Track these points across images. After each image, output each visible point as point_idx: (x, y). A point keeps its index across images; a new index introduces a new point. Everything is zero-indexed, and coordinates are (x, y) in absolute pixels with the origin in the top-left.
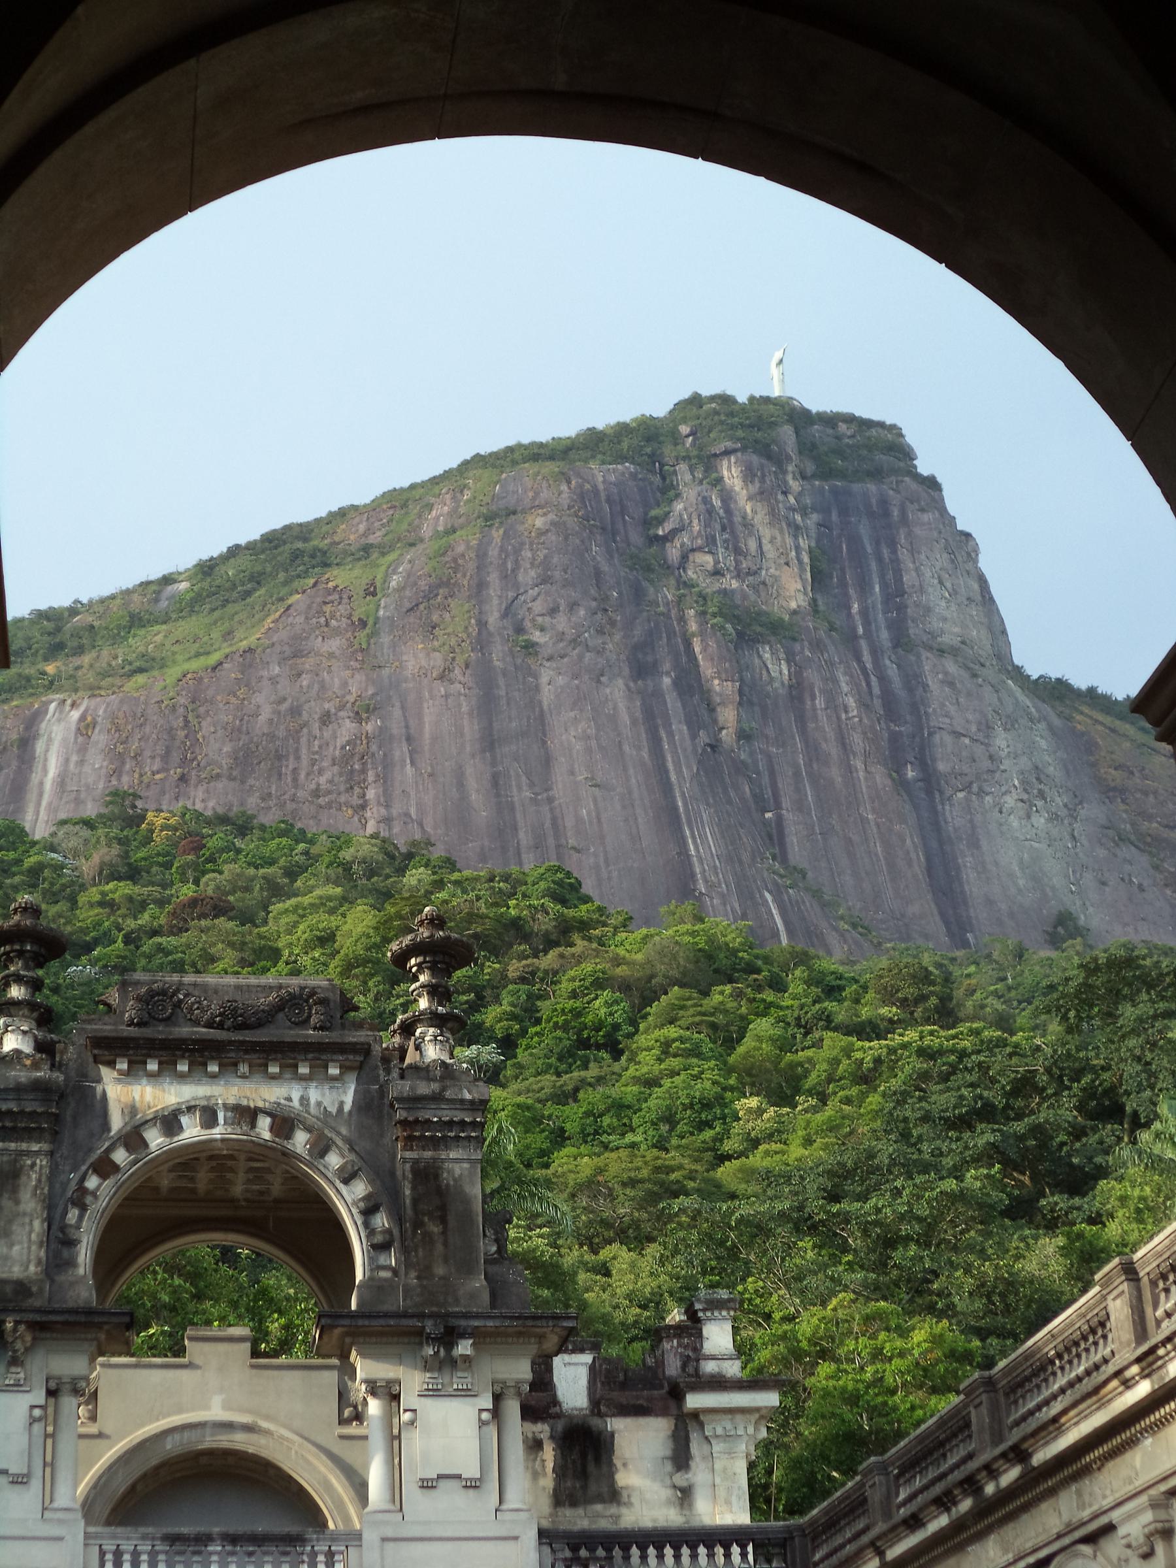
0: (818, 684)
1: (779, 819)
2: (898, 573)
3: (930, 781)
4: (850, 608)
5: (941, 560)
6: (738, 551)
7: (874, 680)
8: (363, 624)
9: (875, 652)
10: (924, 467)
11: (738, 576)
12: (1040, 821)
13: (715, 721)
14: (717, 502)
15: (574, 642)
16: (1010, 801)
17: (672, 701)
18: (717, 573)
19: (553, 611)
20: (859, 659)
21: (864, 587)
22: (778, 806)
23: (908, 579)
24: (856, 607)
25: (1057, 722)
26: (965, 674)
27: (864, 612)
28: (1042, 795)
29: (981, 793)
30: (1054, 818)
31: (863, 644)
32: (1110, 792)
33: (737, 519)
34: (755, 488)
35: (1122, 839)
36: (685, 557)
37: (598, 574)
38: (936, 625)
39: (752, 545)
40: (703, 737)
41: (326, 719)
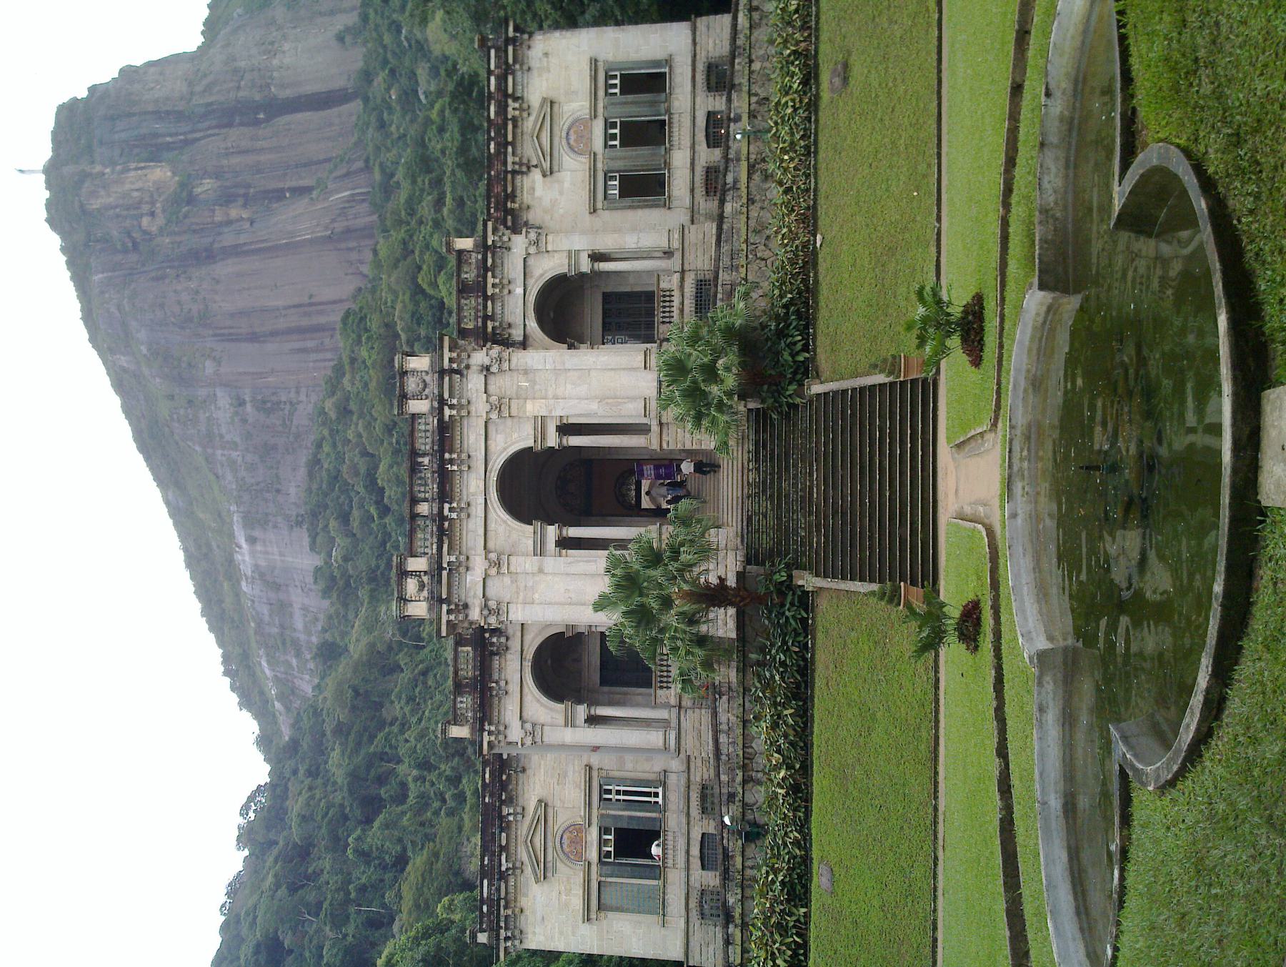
1: (289, 189)
6: (140, 202)
7: (210, 132)
8: (190, 402)
11: (153, 203)
12: (286, 46)
13: (237, 220)
14: (111, 212)
15: (197, 292)
16: (275, 62)
18: (152, 214)
19: (179, 302)
21: (156, 135)
22: (282, 191)
23: (150, 108)
24: (169, 139)
27: (171, 135)
28: (272, 43)
29: (271, 78)
30: (285, 37)
31: (190, 136)
33: (121, 202)
34: (102, 193)
36: (145, 232)
39: (135, 194)
40: (247, 225)
41: (244, 421)
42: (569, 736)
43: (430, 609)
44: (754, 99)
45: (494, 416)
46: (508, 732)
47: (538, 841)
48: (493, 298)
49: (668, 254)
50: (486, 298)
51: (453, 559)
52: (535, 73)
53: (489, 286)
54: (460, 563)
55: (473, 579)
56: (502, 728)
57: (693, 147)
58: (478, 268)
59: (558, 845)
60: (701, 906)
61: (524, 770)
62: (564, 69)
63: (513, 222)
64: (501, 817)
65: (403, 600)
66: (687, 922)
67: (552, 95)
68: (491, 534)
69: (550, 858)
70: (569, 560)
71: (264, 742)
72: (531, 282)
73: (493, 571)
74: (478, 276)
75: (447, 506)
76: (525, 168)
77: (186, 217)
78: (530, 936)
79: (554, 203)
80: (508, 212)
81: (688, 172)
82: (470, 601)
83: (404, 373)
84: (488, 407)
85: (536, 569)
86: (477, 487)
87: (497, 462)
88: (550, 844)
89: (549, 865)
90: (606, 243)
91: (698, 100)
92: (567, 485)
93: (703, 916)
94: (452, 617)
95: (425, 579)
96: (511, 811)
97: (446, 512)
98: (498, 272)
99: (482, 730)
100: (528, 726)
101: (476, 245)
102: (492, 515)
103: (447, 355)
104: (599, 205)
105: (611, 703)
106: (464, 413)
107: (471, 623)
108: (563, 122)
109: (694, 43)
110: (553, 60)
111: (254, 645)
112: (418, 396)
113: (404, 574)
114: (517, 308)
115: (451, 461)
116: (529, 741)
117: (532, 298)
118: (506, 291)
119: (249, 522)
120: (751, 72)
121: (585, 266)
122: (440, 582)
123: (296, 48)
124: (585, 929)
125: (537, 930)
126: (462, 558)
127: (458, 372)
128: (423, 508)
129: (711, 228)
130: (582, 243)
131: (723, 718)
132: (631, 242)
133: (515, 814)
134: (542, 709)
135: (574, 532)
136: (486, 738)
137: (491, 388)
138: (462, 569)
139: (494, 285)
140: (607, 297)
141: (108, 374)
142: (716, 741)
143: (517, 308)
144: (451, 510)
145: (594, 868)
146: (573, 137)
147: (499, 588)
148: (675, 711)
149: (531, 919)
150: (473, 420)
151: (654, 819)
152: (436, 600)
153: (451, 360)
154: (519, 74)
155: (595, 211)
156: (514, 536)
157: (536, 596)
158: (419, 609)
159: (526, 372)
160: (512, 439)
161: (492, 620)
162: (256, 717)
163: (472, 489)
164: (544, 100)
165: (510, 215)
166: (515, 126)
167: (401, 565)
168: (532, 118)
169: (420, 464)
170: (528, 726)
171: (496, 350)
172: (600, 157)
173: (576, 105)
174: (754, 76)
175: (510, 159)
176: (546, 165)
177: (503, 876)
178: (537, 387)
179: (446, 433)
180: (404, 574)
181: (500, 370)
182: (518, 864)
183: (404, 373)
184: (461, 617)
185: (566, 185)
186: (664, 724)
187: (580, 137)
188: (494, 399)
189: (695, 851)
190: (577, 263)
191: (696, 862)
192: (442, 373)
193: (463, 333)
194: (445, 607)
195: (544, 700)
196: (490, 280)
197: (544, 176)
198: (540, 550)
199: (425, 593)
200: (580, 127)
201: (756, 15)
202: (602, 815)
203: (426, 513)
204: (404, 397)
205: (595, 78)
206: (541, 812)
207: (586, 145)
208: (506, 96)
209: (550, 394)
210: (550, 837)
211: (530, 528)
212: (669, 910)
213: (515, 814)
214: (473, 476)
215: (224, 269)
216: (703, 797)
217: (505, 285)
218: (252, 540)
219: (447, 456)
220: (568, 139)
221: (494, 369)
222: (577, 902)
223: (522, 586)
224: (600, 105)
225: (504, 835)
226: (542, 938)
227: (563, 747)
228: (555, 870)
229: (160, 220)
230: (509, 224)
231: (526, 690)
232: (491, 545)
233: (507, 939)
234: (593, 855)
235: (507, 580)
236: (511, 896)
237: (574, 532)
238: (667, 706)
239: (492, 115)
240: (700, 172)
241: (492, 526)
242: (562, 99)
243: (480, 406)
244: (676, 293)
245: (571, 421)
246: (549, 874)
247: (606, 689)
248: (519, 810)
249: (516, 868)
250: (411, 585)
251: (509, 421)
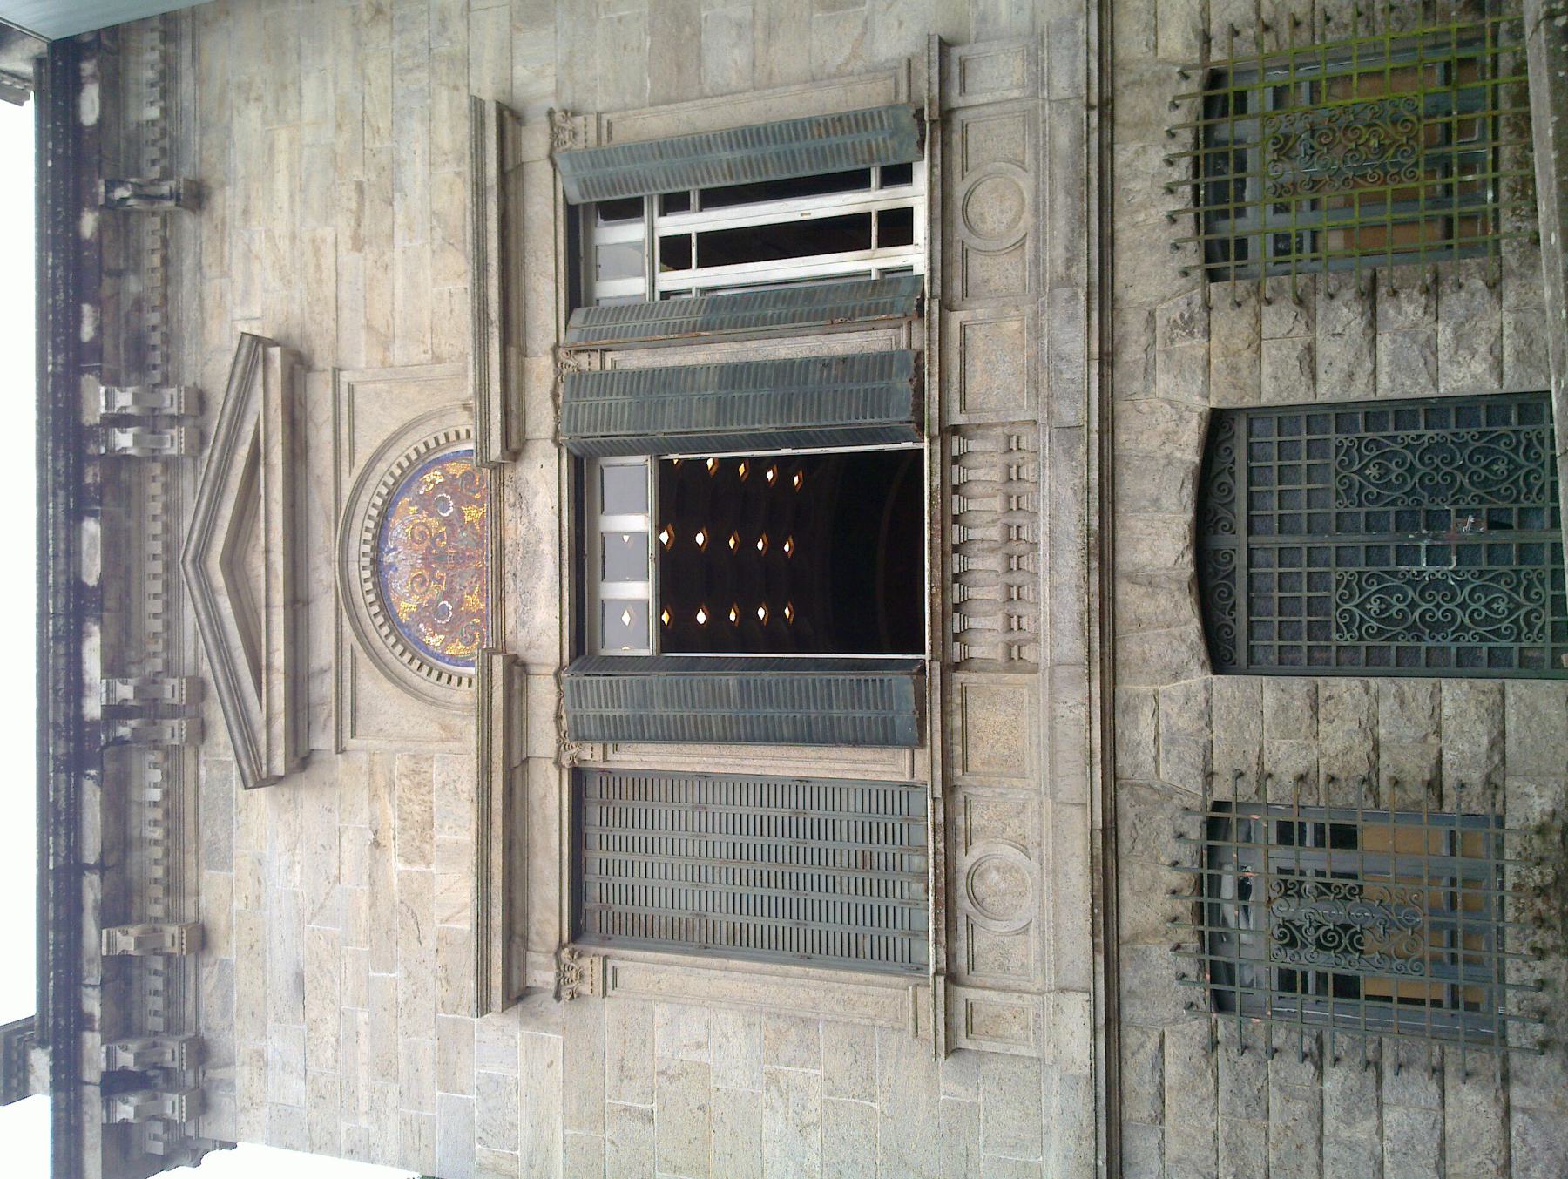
59: (359, 572)
60: (1206, 913)
61: (196, 197)
66: (1111, 1025)
69: (323, 652)
78: (243, 1075)
89: (324, 689)
96: (124, 399)
124: (502, 1044)
125: (276, 1045)
145: (543, 693)
151: (880, 363)
182: (172, 691)
189: (1159, 540)
191: (1164, 620)
202: (578, 383)
210: (322, 535)
212: (988, 939)
213: (149, 421)
216: (1214, 178)
228: (349, 716)
233: (116, 1083)
236: (150, 863)
246: (323, 741)
248: (171, 400)
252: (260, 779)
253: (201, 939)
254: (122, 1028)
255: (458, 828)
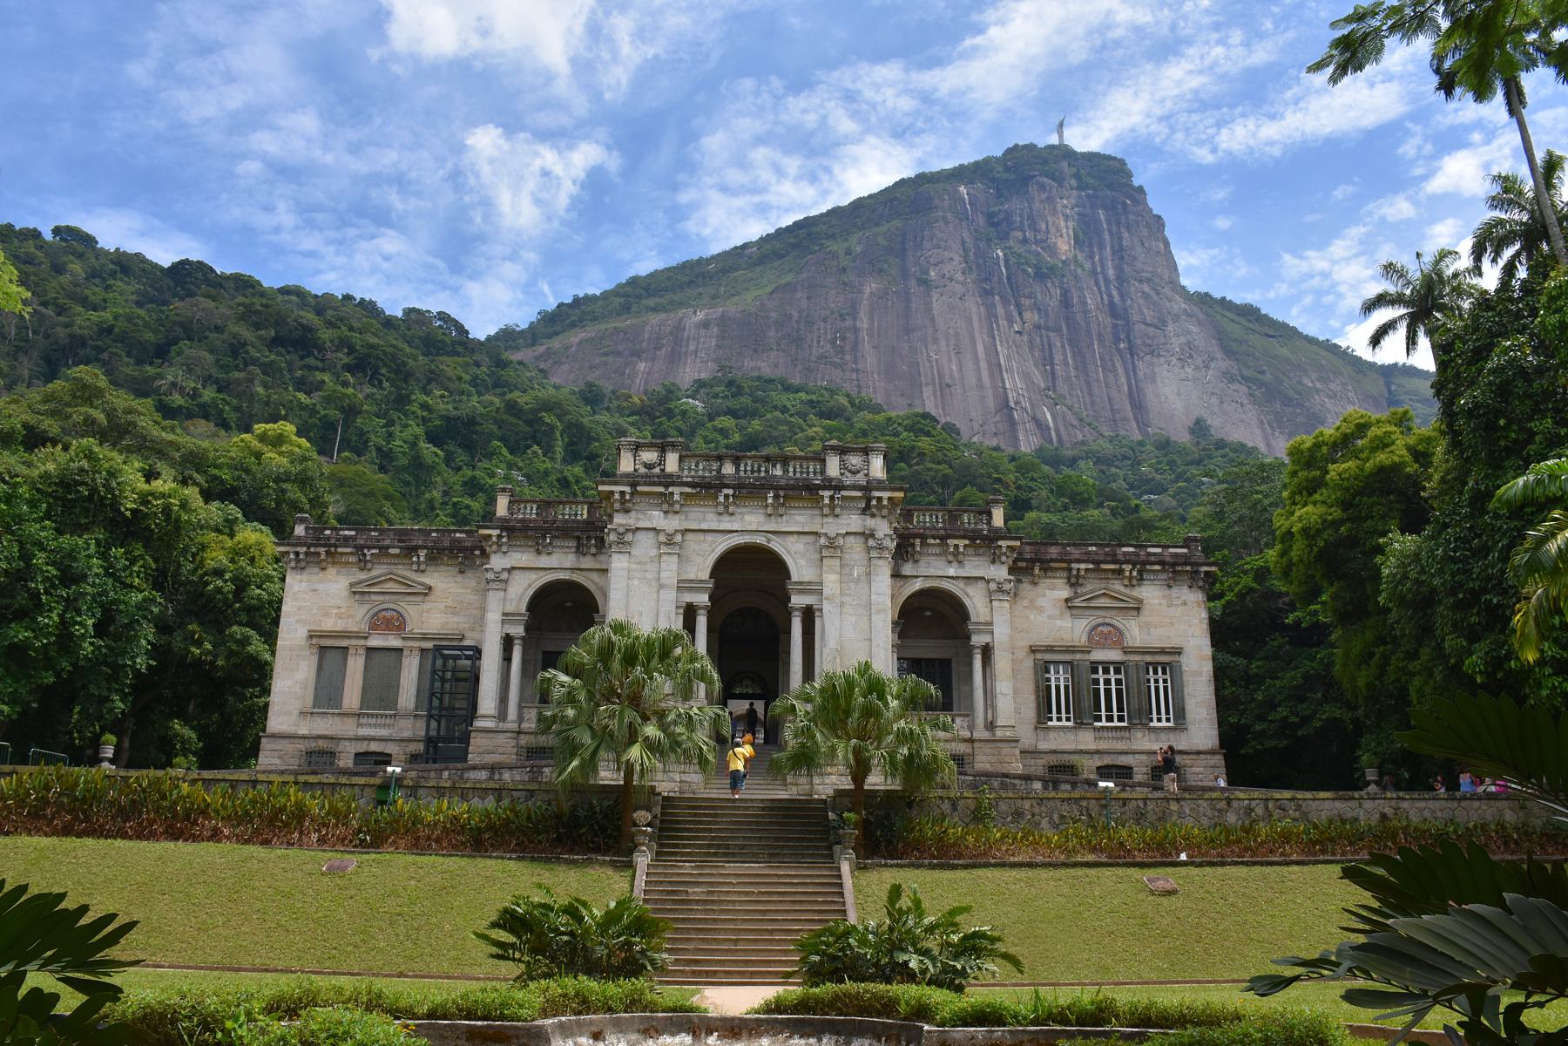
0: (1075, 300)
1: (1052, 369)
2: (1120, 239)
3: (1132, 350)
4: (1092, 257)
5: (1145, 232)
6: (1036, 230)
9: (1107, 281)
10: (1136, 182)
11: (1037, 243)
12: (1189, 370)
17: (1000, 311)
20: (1097, 284)
21: (1101, 247)
22: (1052, 364)
25: (1202, 317)
26: (1153, 294)
27: (1101, 260)
30: (1197, 368)
31: (1100, 277)
32: (1229, 353)
34: (1043, 196)
35: (1232, 380)
36: (1008, 233)
37: (963, 243)
38: (1139, 265)
39: (1044, 227)
42: (493, 617)
43: (628, 475)
44: (1141, 804)
45: (823, 541)
46: (499, 555)
47: (391, 585)
48: (943, 544)
49: (991, 726)
50: (943, 538)
51: (676, 497)
52: (1167, 592)
53: (956, 542)
54: (672, 505)
55: (656, 518)
56: (504, 549)
57: (1098, 752)
58: (974, 531)
62: (1175, 621)
63: (1021, 568)
64: (416, 549)
65: (637, 448)
66: (304, 737)
67: (1145, 611)
68: (701, 536)
69: (374, 597)
70: (673, 616)
71: (507, 336)
72: (961, 584)
73: (662, 538)
74: (965, 530)
75: (730, 492)
76: (1074, 582)
77: (1024, 271)
79: (1041, 610)
80: (1032, 561)
81: (1071, 747)
82: (633, 514)
83: (866, 452)
84: (832, 535)
85: (663, 581)
86: (750, 524)
87: (776, 545)
88: (387, 598)
90: (1001, 662)
91: (1144, 757)
92: (751, 616)
93: (309, 753)
94: (617, 496)
95: (657, 470)
97: (726, 491)
98: (970, 551)
99: (502, 529)
100: (505, 576)
101: (998, 530)
102: (720, 538)
103: (885, 495)
104: (1039, 656)
105: (524, 661)
106: (826, 511)
107: (611, 517)
108: (1119, 621)
109: (1199, 753)
110: (1180, 609)
111: (603, 327)
112: (843, 466)
113: (663, 450)
114: (934, 570)
115: (776, 497)
116: (490, 576)
117: (944, 585)
118: (950, 558)
119: (723, 321)
120: (1167, 800)
121: (978, 640)
122: (654, 484)
123: (1187, 380)
124: (302, 633)
126: (677, 507)
127: (868, 507)
128: (728, 469)
129: (1017, 767)
130: (1001, 634)
131: (507, 776)
132: (1003, 687)
133: (419, 563)
134: (521, 590)
135: (702, 622)
136: (495, 532)
137: (851, 539)
138: (665, 507)
139: (956, 546)
140: (946, 664)
141: (870, 196)
142: (483, 767)
143: (934, 570)
144: (726, 496)
145: (362, 642)
146: (1105, 629)
147: (644, 546)
148: (514, 726)
149: (315, 578)
150: (818, 520)
152: (633, 480)
153: (880, 499)
154: (1165, 576)
155: (1033, 651)
156: (699, 560)
157: (636, 582)
158: (626, 464)
159: (869, 574)
160: (799, 563)
161: (613, 537)
162: (532, 326)
163: (747, 518)
164: (1141, 601)
165: (1027, 567)
166: (1113, 571)
167: (673, 446)
168: (1122, 589)
169: (774, 466)
170: (505, 576)
171: (892, 545)
172: (1087, 657)
173: (1137, 633)
174: (1165, 804)
175: (1083, 566)
176: (1077, 602)
177: (360, 548)
178: (852, 586)
179: (805, 492)
180: (663, 450)
181: (869, 549)
182: (369, 565)
183: (866, 452)
184: (617, 506)
185: (1058, 623)
186: (502, 715)
187: (1106, 636)
188: (841, 541)
189: (374, 747)
190: (979, 632)
191: (362, 747)
192: (867, 488)
193: (907, 516)
194: (627, 489)
195: (531, 592)
196: (962, 543)
197: (1067, 600)
198: (683, 586)
199: (643, 470)
200: (1114, 637)
201: (1223, 805)
203: (724, 471)
204: (843, 451)
205: (1163, 651)
206: (420, 589)
207: (1098, 643)
208: (1144, 563)
209: (846, 599)
211: (705, 575)
212: (318, 719)
214: (762, 518)
215: (973, 307)
217: (957, 557)
218: (705, 325)
219: (782, 493)
220: (1103, 624)
221: (871, 542)
222: (329, 625)
223: (648, 567)
224: (1137, 658)
225: (397, 551)
226: (296, 589)
227: (483, 610)
228: (362, 603)
229: (1019, 249)
230: (1021, 564)
231: (541, 573)
232: (689, 536)
233: (297, 554)
234: (375, 642)
235: (654, 552)
237: (702, 622)
238: (521, 719)
239: (1125, 549)
240: (1074, 759)
241: (709, 537)
242: (1142, 619)
243: (832, 527)
244: (948, 735)
245: (817, 621)
247: (540, 657)
248: (423, 567)
249: (363, 564)
250: (650, 456)
251: (817, 556)
252: (351, 585)
253: (323, 569)
254: (307, 554)
255: (339, 626)
